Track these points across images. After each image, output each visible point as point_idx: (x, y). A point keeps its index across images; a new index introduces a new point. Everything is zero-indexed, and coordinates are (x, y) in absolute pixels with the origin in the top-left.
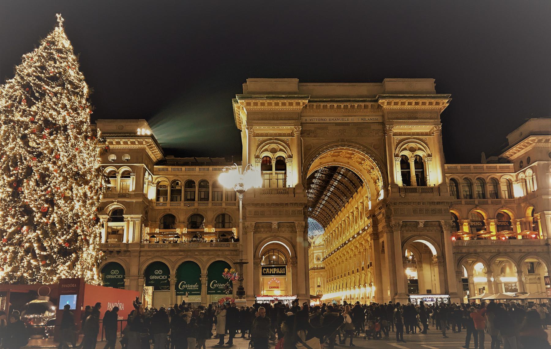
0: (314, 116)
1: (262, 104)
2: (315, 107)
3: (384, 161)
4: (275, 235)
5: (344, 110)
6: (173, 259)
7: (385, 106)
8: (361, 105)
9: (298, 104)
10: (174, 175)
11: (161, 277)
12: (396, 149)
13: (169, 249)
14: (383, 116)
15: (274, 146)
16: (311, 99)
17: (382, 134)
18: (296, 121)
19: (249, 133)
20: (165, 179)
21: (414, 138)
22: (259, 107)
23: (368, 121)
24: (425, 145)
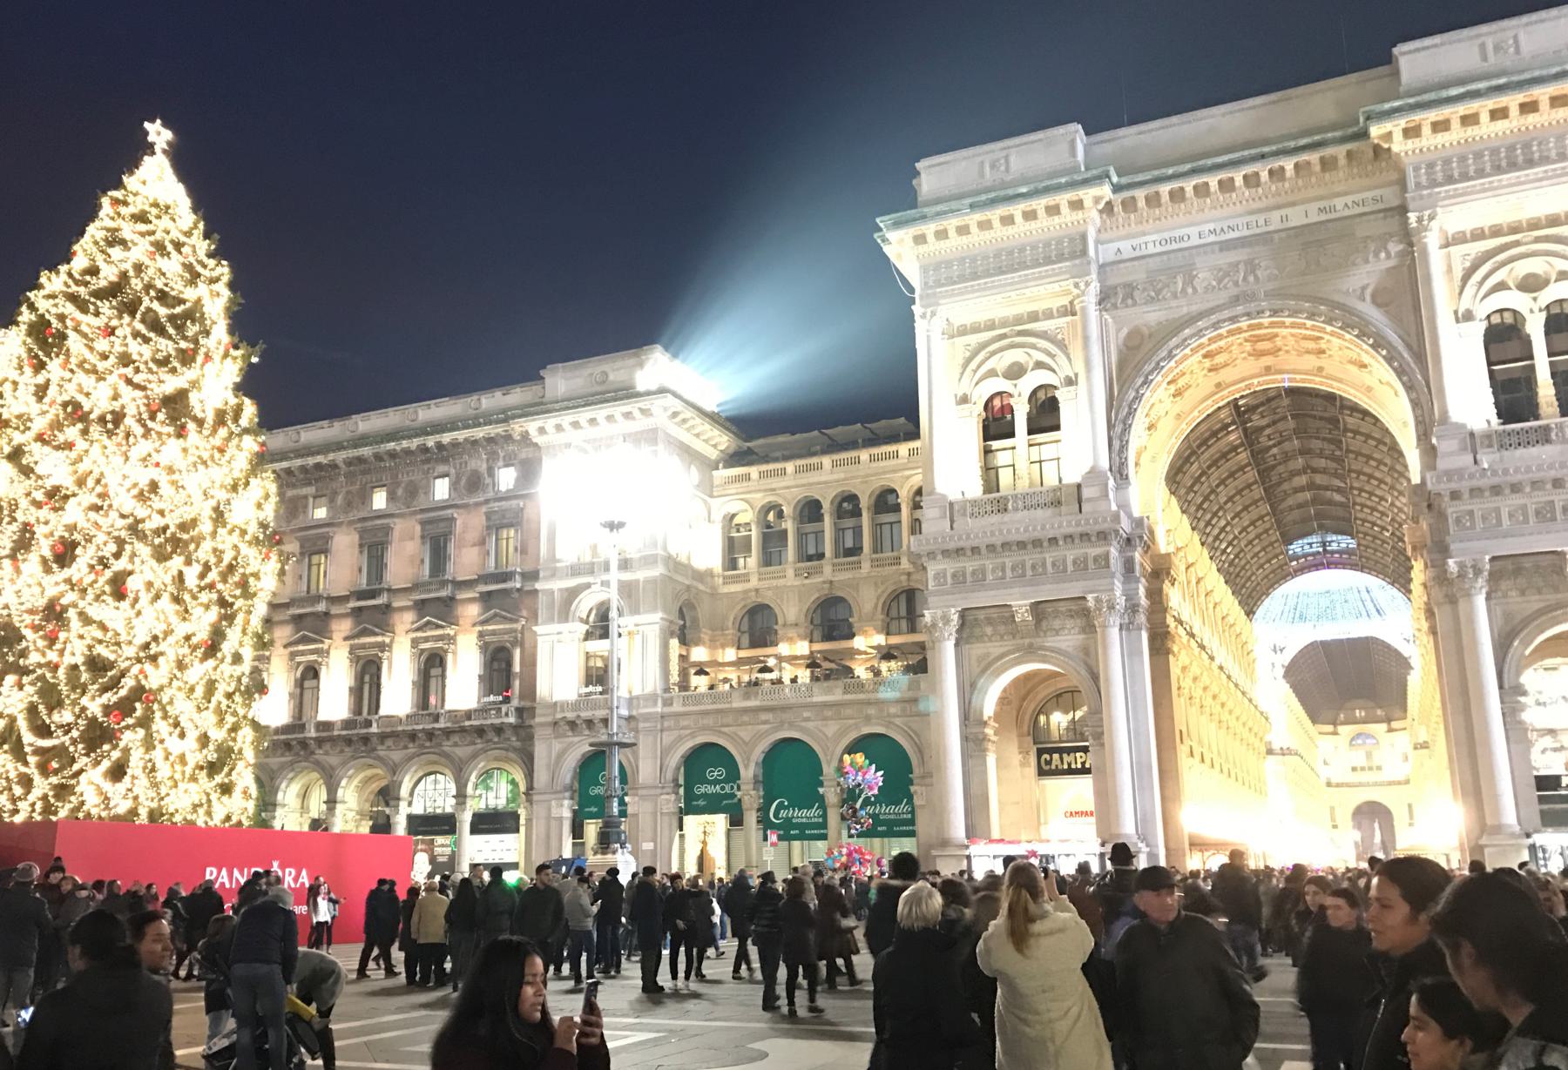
0: (1144, 234)
2: (1141, 203)
3: (1415, 347)
4: (1031, 646)
5: (1247, 193)
6: (745, 733)
7: (1398, 145)
8: (1308, 163)
9: (1077, 205)
10: (765, 490)
11: (723, 789)
13: (735, 705)
14: (1402, 183)
16: (1124, 180)
17: (1401, 247)
18: (1077, 262)
20: (745, 506)
21: (1537, 240)
23: (1347, 213)
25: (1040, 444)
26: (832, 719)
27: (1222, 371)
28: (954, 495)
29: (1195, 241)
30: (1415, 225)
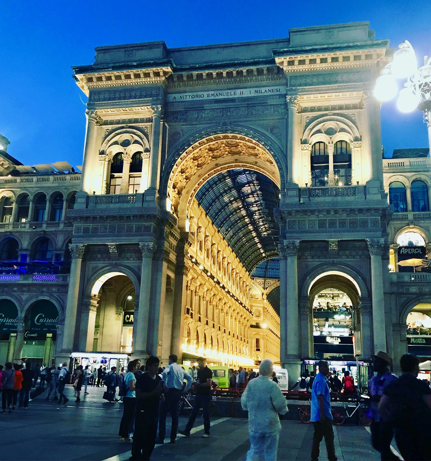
0: (185, 92)
1: (109, 78)
2: (185, 79)
3: (285, 153)
4: (116, 264)
7: (286, 68)
8: (252, 71)
9: (157, 74)
12: (304, 133)
15: (126, 137)
18: (155, 98)
19: (89, 120)
21: (334, 114)
22: (105, 83)
23: (265, 94)
24: (351, 124)
25: (134, 177)
26: (26, 292)
27: (219, 159)
28: (90, 193)
29: (206, 98)
30: (289, 101)
